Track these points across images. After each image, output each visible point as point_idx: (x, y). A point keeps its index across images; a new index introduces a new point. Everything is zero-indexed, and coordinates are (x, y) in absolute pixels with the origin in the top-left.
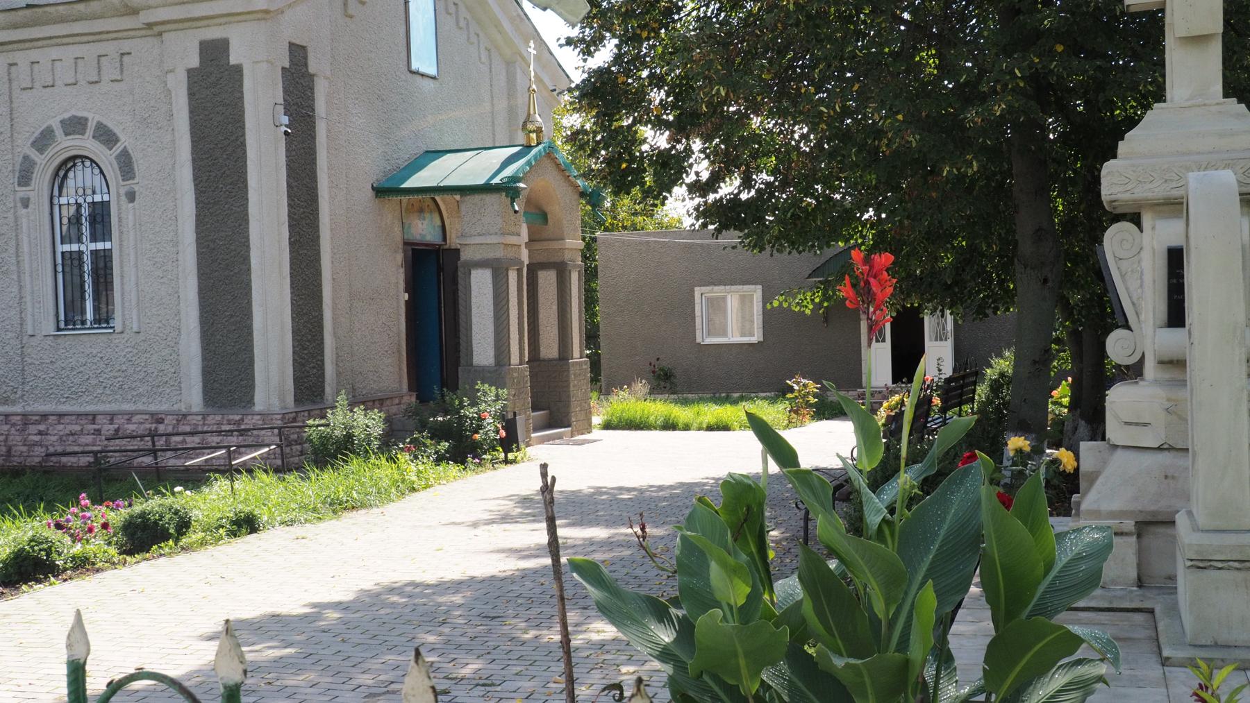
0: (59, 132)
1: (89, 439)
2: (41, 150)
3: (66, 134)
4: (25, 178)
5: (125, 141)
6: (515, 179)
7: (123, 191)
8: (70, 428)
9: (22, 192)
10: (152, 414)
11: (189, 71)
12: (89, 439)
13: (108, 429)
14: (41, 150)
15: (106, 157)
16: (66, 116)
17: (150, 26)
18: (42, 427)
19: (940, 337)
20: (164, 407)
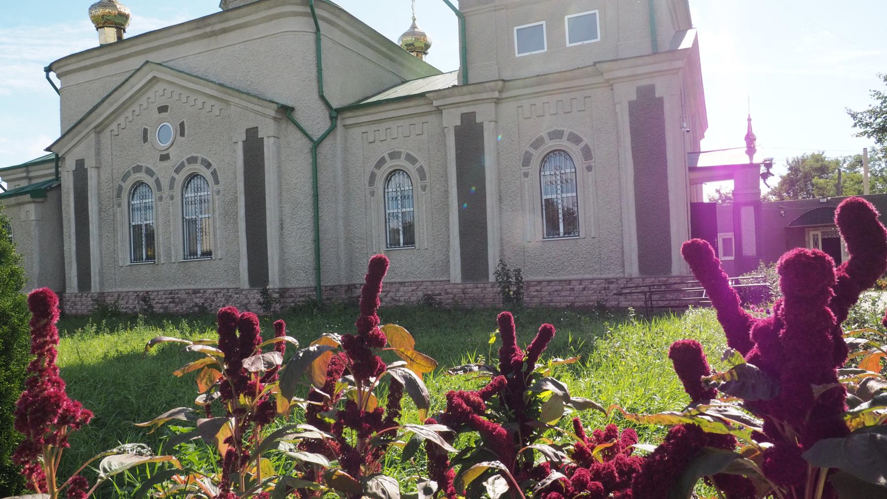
0: (546, 139)
1: (568, 293)
2: (536, 148)
3: (551, 139)
4: (526, 162)
5: (586, 140)
7: (584, 166)
8: (554, 288)
9: (525, 169)
10: (606, 279)
11: (630, 103)
12: (568, 293)
13: (578, 287)
14: (536, 148)
15: (576, 151)
16: (551, 130)
17: (607, 81)
18: (538, 288)
20: (611, 276)
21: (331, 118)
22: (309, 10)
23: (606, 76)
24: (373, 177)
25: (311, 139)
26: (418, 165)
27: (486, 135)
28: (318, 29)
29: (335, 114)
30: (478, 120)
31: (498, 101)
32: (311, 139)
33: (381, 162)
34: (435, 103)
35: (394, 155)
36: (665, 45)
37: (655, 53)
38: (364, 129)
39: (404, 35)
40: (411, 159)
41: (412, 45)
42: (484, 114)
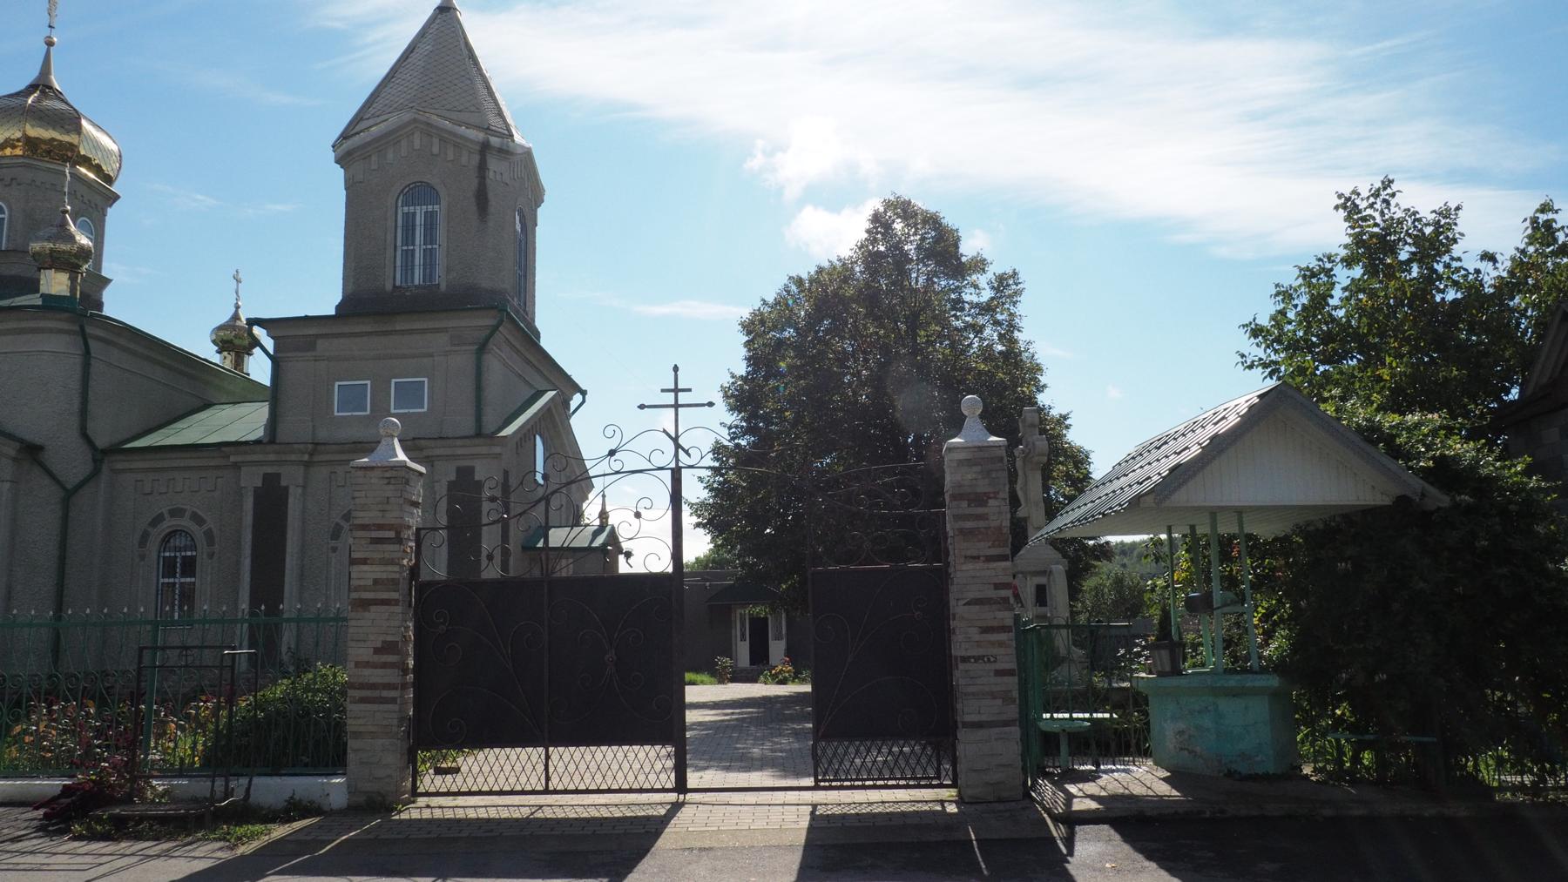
6: (604, 545)
19: (778, 638)
21: (95, 461)
22: (76, 328)
23: (425, 453)
24: (145, 537)
25: (64, 488)
26: (205, 528)
27: (291, 500)
28: (87, 352)
29: (102, 456)
30: (283, 483)
31: (308, 465)
32: (64, 488)
33: (158, 520)
34: (232, 459)
35: (176, 513)
36: (489, 427)
37: (479, 435)
38: (139, 476)
39: (220, 328)
40: (196, 518)
41: (230, 342)
42: (291, 476)
